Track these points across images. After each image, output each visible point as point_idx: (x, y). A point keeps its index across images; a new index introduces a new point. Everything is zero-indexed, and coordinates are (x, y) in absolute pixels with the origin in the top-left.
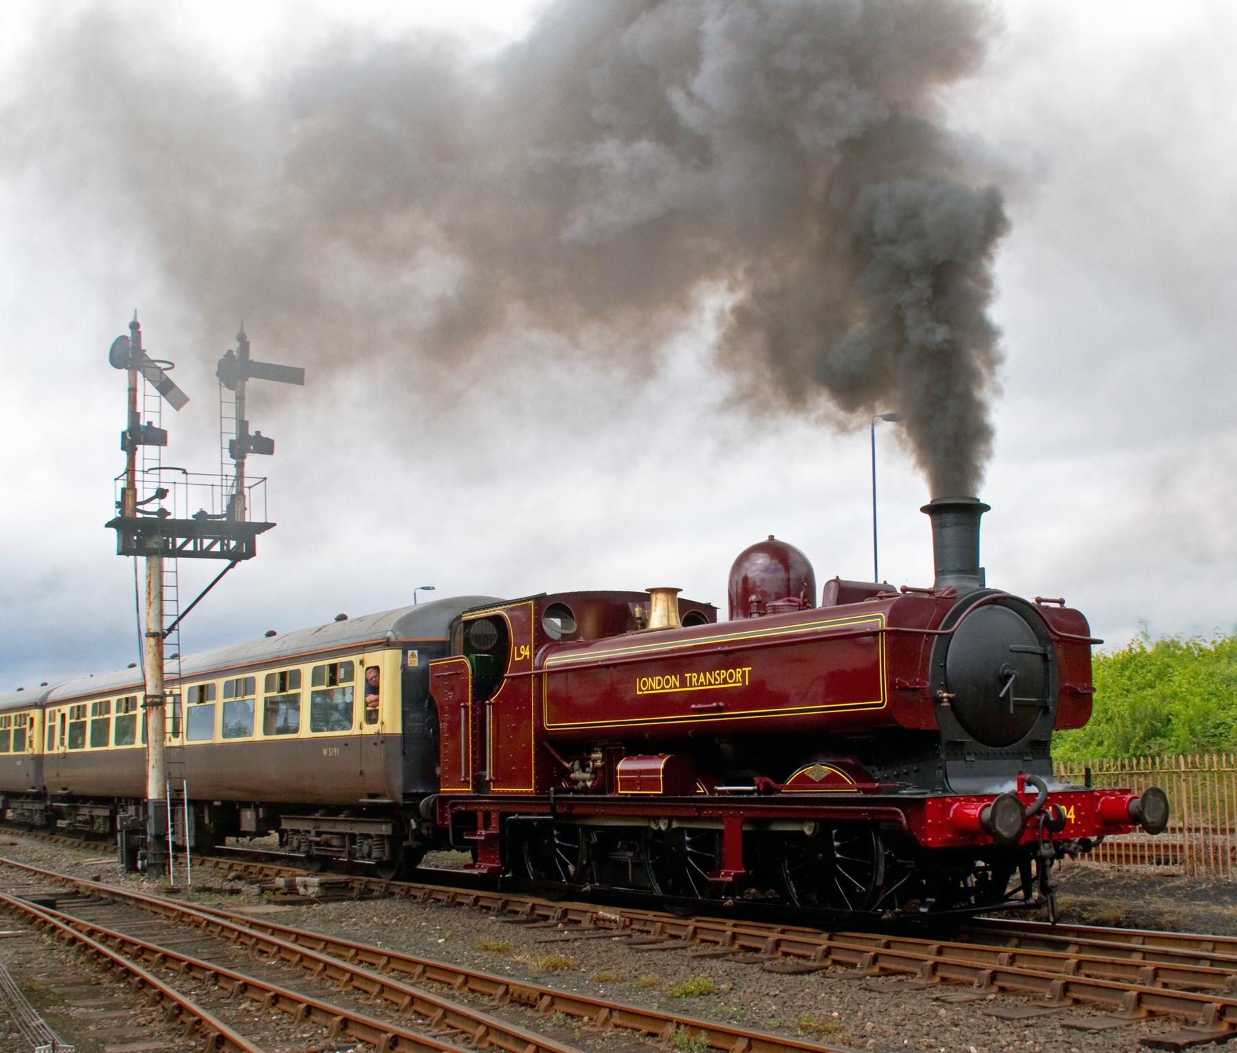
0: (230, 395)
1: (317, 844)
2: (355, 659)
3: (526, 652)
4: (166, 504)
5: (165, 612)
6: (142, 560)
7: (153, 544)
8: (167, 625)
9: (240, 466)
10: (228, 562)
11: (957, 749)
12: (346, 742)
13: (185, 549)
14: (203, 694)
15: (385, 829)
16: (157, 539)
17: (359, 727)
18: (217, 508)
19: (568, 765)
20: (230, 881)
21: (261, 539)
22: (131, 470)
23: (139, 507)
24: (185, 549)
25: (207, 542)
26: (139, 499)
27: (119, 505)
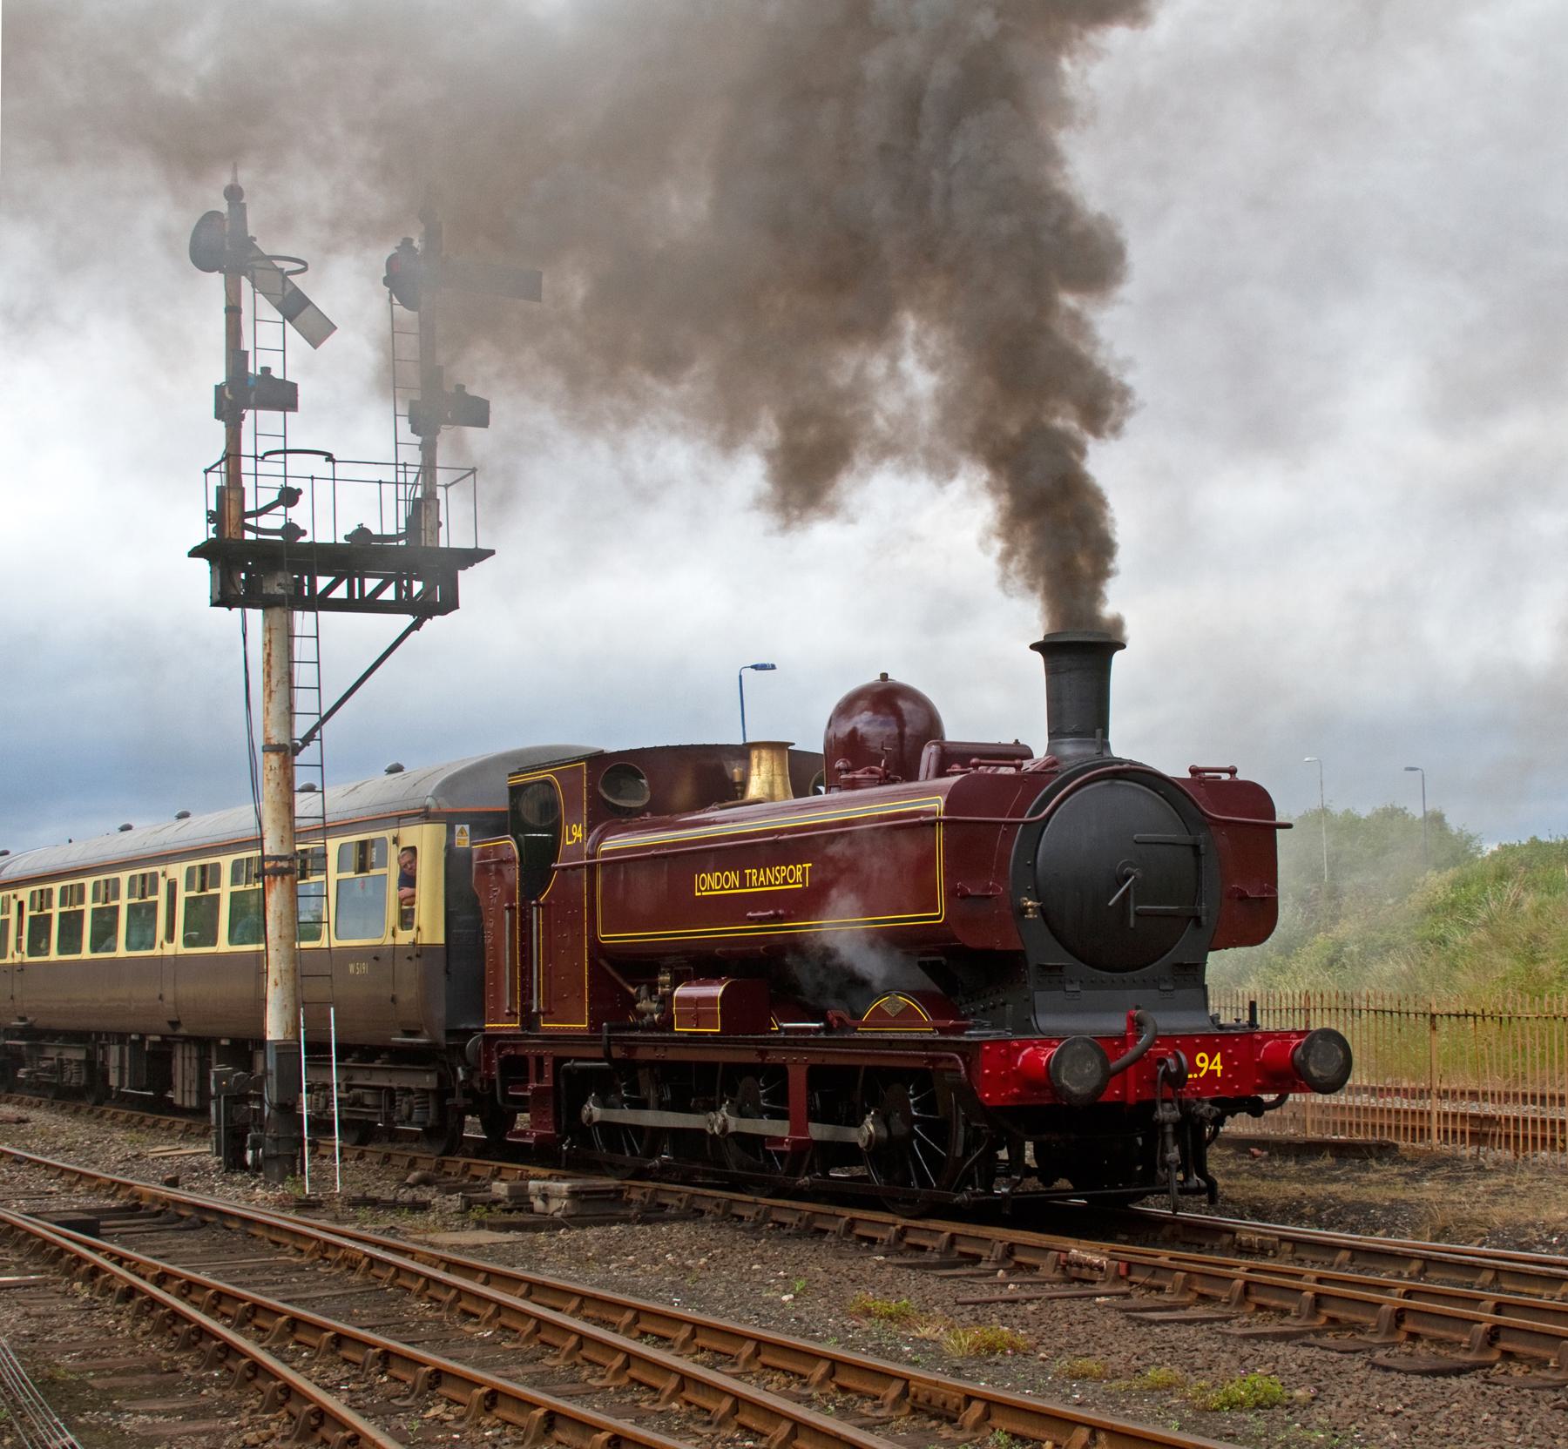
4: (299, 514)
5: (297, 710)
6: (255, 616)
7: (274, 587)
10: (407, 620)
11: (1052, 975)
13: (334, 595)
14: (363, 858)
16: (280, 577)
18: (387, 521)
19: (633, 991)
20: (411, 1186)
21: (468, 580)
22: (232, 456)
23: (250, 521)
24: (334, 595)
26: (249, 506)
27: (212, 517)
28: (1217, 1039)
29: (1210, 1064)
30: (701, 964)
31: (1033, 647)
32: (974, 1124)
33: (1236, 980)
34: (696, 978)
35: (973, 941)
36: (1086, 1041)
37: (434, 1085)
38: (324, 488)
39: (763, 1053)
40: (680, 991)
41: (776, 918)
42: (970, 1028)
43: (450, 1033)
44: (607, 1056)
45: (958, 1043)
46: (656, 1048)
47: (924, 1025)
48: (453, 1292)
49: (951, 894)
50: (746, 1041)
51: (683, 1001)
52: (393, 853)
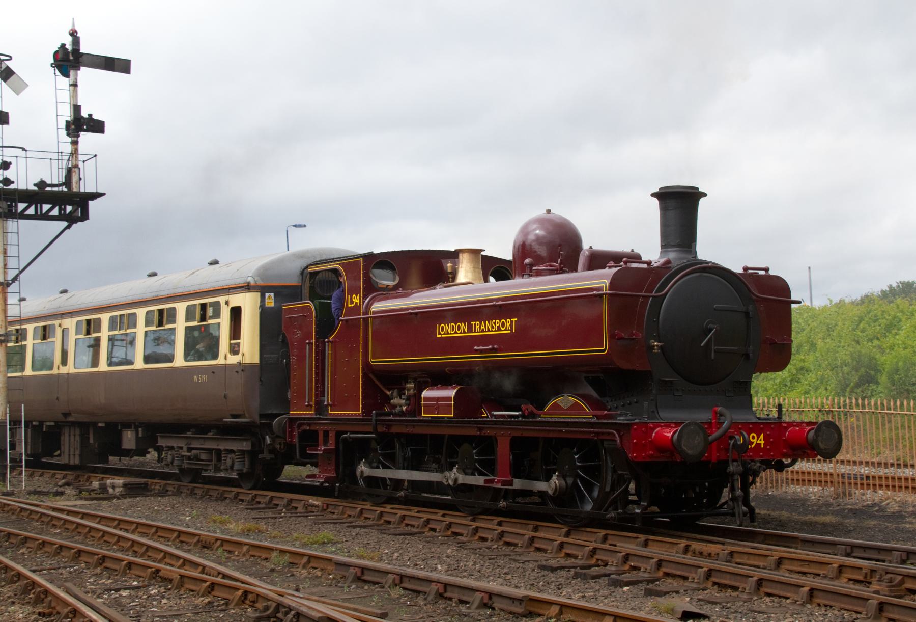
0: (64, 82)
1: (189, 458)
2: (222, 299)
3: (356, 300)
5: (9, 266)
8: (10, 276)
9: (75, 143)
10: (65, 224)
12: (213, 370)
14: (45, 333)
15: (246, 446)
17: (225, 358)
21: (93, 206)
25: (46, 207)
28: (760, 426)
29: (758, 440)
30: (440, 378)
31: (653, 195)
32: (620, 472)
33: (767, 393)
34: (436, 385)
35: (624, 365)
36: (696, 424)
37: (249, 448)
38: (22, 161)
39: (480, 429)
40: (426, 393)
41: (495, 350)
42: (620, 415)
43: (262, 416)
44: (375, 431)
45: (616, 424)
46: (414, 426)
47: (587, 414)
48: (145, 548)
49: (612, 336)
50: (469, 422)
51: (426, 399)
52: (59, 332)
